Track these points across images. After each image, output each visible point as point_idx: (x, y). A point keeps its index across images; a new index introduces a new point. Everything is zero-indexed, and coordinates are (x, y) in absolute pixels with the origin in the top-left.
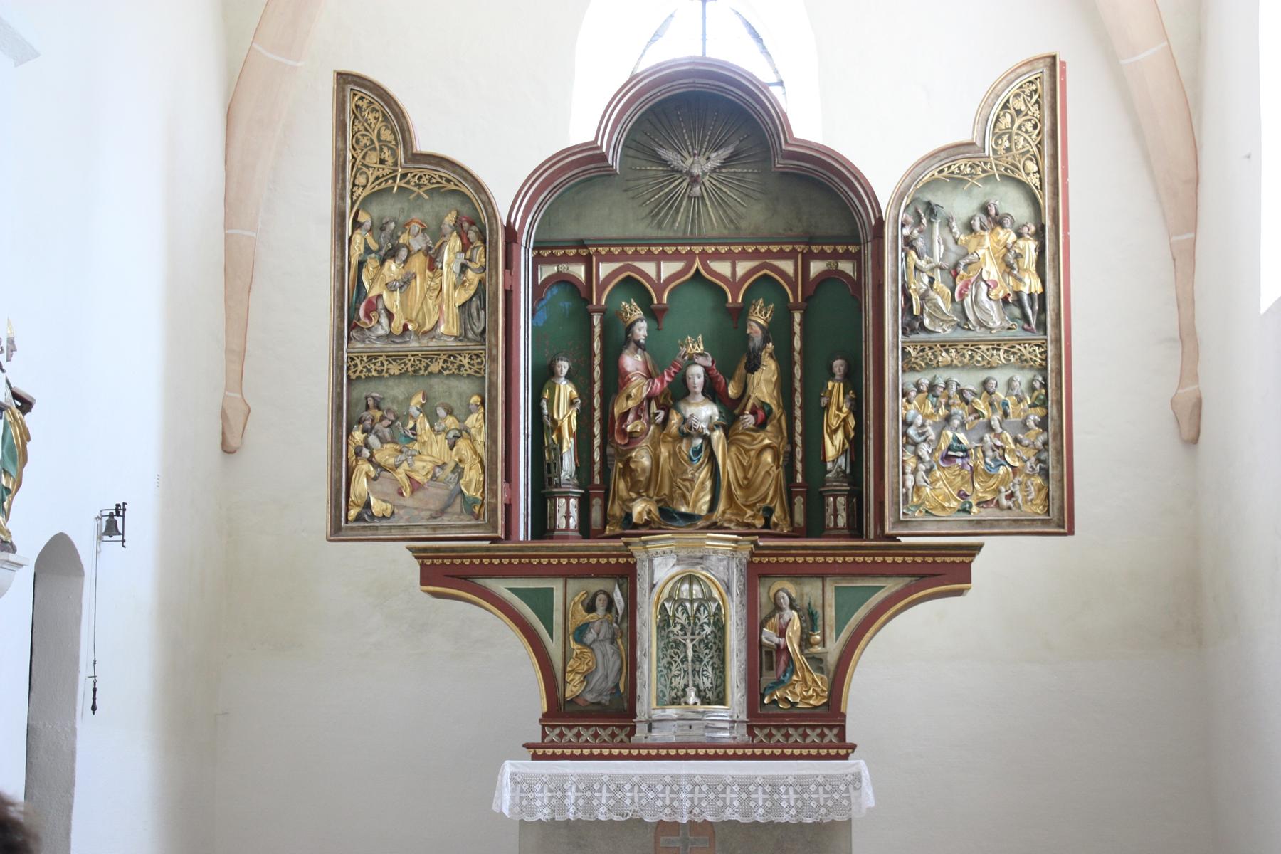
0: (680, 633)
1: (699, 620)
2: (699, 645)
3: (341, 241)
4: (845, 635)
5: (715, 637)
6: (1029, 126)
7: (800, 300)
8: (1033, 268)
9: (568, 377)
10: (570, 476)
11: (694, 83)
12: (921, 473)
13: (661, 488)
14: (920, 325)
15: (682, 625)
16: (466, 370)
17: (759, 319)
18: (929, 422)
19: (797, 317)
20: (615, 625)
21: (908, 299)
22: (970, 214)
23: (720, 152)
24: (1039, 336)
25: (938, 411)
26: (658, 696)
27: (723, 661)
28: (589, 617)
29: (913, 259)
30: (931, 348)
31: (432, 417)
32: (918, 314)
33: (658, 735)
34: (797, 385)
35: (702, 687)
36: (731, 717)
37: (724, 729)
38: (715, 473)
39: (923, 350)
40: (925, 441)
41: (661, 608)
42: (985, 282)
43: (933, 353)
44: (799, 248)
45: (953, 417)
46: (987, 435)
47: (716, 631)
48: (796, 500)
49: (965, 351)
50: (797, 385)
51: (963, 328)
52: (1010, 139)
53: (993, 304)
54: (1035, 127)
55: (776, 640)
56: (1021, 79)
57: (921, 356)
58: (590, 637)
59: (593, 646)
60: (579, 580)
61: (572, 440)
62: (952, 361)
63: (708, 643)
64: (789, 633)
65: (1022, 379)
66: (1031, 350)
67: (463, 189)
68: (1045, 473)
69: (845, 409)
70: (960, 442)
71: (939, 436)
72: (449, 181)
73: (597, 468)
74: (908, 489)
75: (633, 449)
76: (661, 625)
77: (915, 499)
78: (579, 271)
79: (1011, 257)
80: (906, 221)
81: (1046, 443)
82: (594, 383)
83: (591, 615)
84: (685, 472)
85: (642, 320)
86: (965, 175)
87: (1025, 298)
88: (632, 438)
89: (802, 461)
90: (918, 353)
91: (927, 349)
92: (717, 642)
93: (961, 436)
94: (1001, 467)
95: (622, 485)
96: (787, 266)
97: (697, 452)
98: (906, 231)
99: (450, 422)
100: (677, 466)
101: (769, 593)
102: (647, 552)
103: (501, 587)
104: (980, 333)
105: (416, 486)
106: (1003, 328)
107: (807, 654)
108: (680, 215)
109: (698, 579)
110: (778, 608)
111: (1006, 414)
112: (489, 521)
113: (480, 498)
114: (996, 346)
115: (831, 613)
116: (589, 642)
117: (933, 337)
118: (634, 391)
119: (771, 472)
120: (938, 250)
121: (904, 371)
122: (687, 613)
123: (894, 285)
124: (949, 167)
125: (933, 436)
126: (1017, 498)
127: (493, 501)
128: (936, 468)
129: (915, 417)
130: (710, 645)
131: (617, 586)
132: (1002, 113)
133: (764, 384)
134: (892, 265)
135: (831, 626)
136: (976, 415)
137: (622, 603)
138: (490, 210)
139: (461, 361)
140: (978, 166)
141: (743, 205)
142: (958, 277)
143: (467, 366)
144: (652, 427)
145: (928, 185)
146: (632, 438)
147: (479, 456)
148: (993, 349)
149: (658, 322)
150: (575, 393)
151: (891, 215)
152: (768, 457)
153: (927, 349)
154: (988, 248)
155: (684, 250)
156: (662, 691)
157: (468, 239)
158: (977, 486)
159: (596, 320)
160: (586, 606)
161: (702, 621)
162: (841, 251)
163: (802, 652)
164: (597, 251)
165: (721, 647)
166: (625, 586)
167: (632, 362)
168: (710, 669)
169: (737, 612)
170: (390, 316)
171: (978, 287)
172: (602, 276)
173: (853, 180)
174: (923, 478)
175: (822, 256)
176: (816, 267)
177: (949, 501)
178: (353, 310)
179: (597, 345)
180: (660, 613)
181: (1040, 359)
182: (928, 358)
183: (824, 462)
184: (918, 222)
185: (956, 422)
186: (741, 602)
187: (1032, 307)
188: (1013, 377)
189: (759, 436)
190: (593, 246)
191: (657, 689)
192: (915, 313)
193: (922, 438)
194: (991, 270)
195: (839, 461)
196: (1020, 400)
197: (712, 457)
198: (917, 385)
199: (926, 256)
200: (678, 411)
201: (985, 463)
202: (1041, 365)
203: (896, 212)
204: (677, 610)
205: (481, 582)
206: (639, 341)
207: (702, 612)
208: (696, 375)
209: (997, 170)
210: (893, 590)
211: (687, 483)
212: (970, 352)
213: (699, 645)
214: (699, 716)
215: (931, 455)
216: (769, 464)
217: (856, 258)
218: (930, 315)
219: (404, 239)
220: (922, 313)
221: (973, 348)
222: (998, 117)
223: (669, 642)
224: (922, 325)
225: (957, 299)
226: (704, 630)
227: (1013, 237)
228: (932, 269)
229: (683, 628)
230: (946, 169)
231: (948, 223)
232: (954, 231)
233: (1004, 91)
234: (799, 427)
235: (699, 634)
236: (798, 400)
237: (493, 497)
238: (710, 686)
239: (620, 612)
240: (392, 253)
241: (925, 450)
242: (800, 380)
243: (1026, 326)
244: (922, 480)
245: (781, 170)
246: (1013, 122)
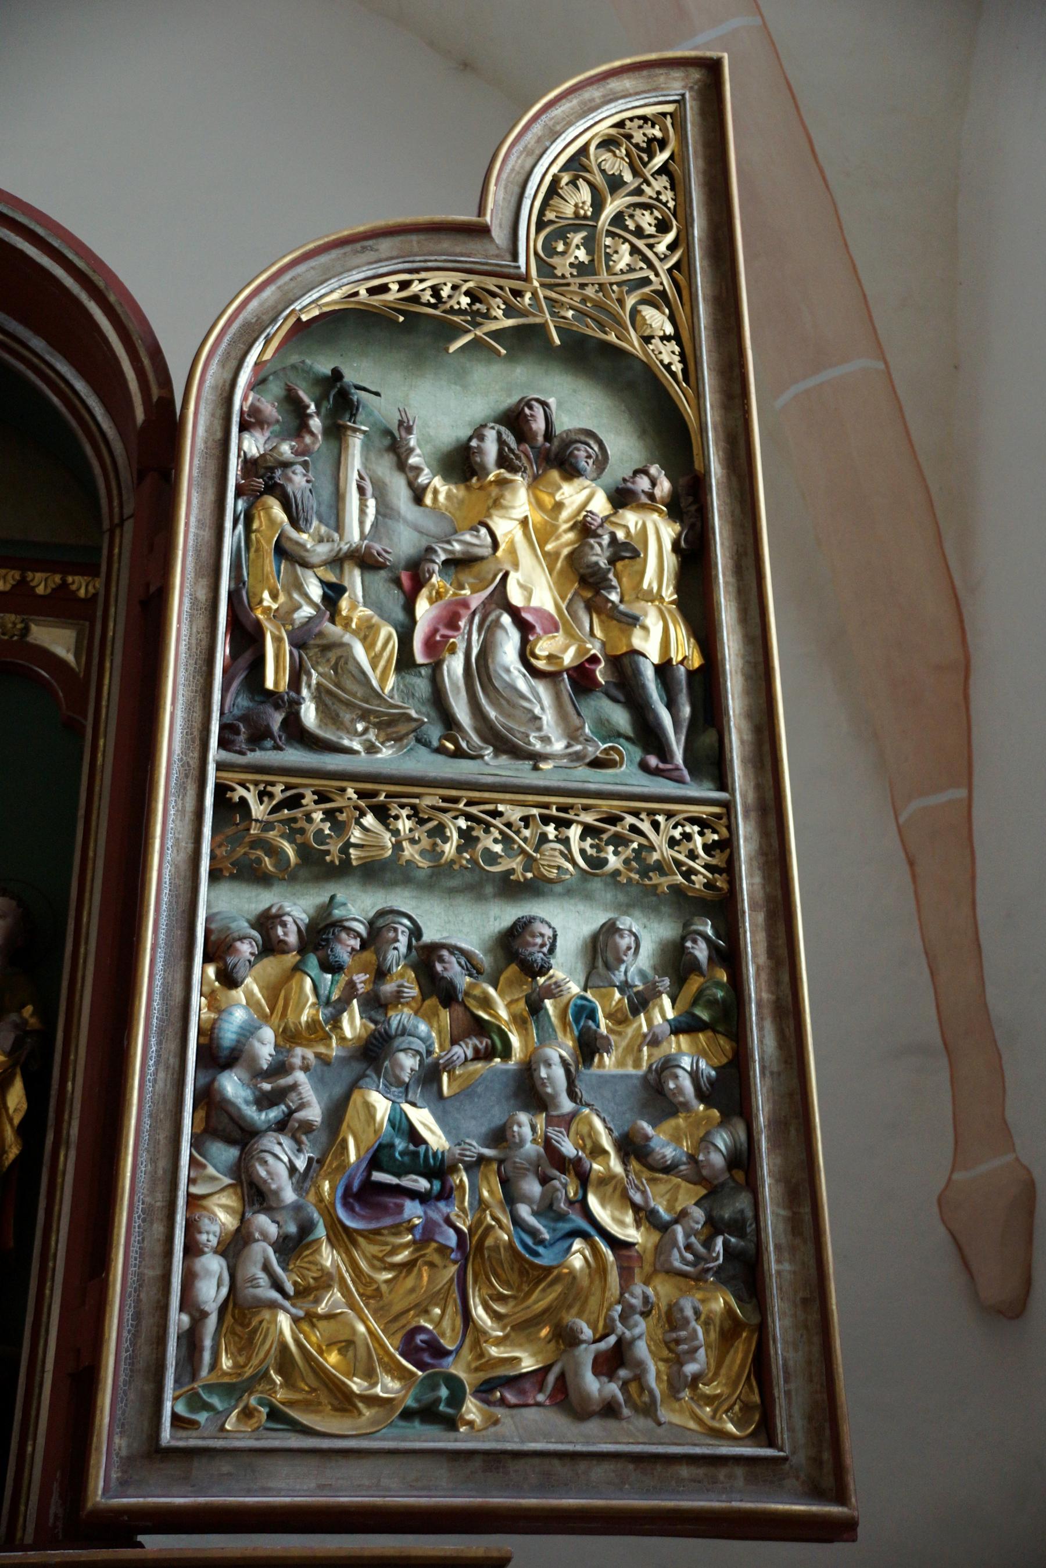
6: (647, 220)
8: (669, 594)
12: (263, 1251)
14: (284, 723)
22: (464, 433)
25: (335, 1022)
29: (272, 521)
30: (322, 798)
39: (294, 802)
40: (281, 1126)
42: (515, 613)
43: (330, 815)
45: (398, 1042)
46: (523, 1117)
49: (446, 818)
51: (441, 750)
52: (589, 244)
53: (542, 688)
54: (663, 227)
56: (620, 105)
62: (398, 847)
66: (677, 833)
70: (414, 1136)
74: (199, 1316)
77: (226, 1363)
79: (599, 555)
80: (255, 411)
86: (452, 311)
87: (649, 674)
90: (275, 810)
91: (309, 799)
93: (422, 1118)
94: (578, 1244)
98: (253, 445)
106: (577, 757)
114: (554, 812)
121: (215, 876)
123: (204, 582)
125: (314, 1113)
126: (639, 1366)
128: (321, 1232)
129: (248, 1032)
132: (566, 178)
134: (201, 524)
136: (482, 1044)
140: (494, 295)
142: (425, 592)
148: (546, 820)
151: (209, 381)
153: (309, 799)
154: (524, 522)
158: (479, 1313)
162: (40, 590)
171: (490, 631)
173: (84, 297)
174: (266, 1268)
177: (370, 1375)
181: (706, 866)
182: (311, 829)
184: (300, 426)
187: (671, 705)
188: (616, 919)
192: (270, 684)
193: (274, 1114)
196: (641, 1003)
199: (315, 523)
201: (517, 1221)
202: (709, 885)
203: (228, 375)
209: (553, 314)
212: (462, 823)
215: (302, 1180)
218: (321, 696)
220: (295, 684)
221: (473, 810)
222: (556, 181)
225: (420, 658)
227: (600, 505)
228: (337, 562)
230: (395, 287)
232: (413, 460)
233: (570, 124)
243: (653, 761)
244: (263, 1279)
246: (598, 205)
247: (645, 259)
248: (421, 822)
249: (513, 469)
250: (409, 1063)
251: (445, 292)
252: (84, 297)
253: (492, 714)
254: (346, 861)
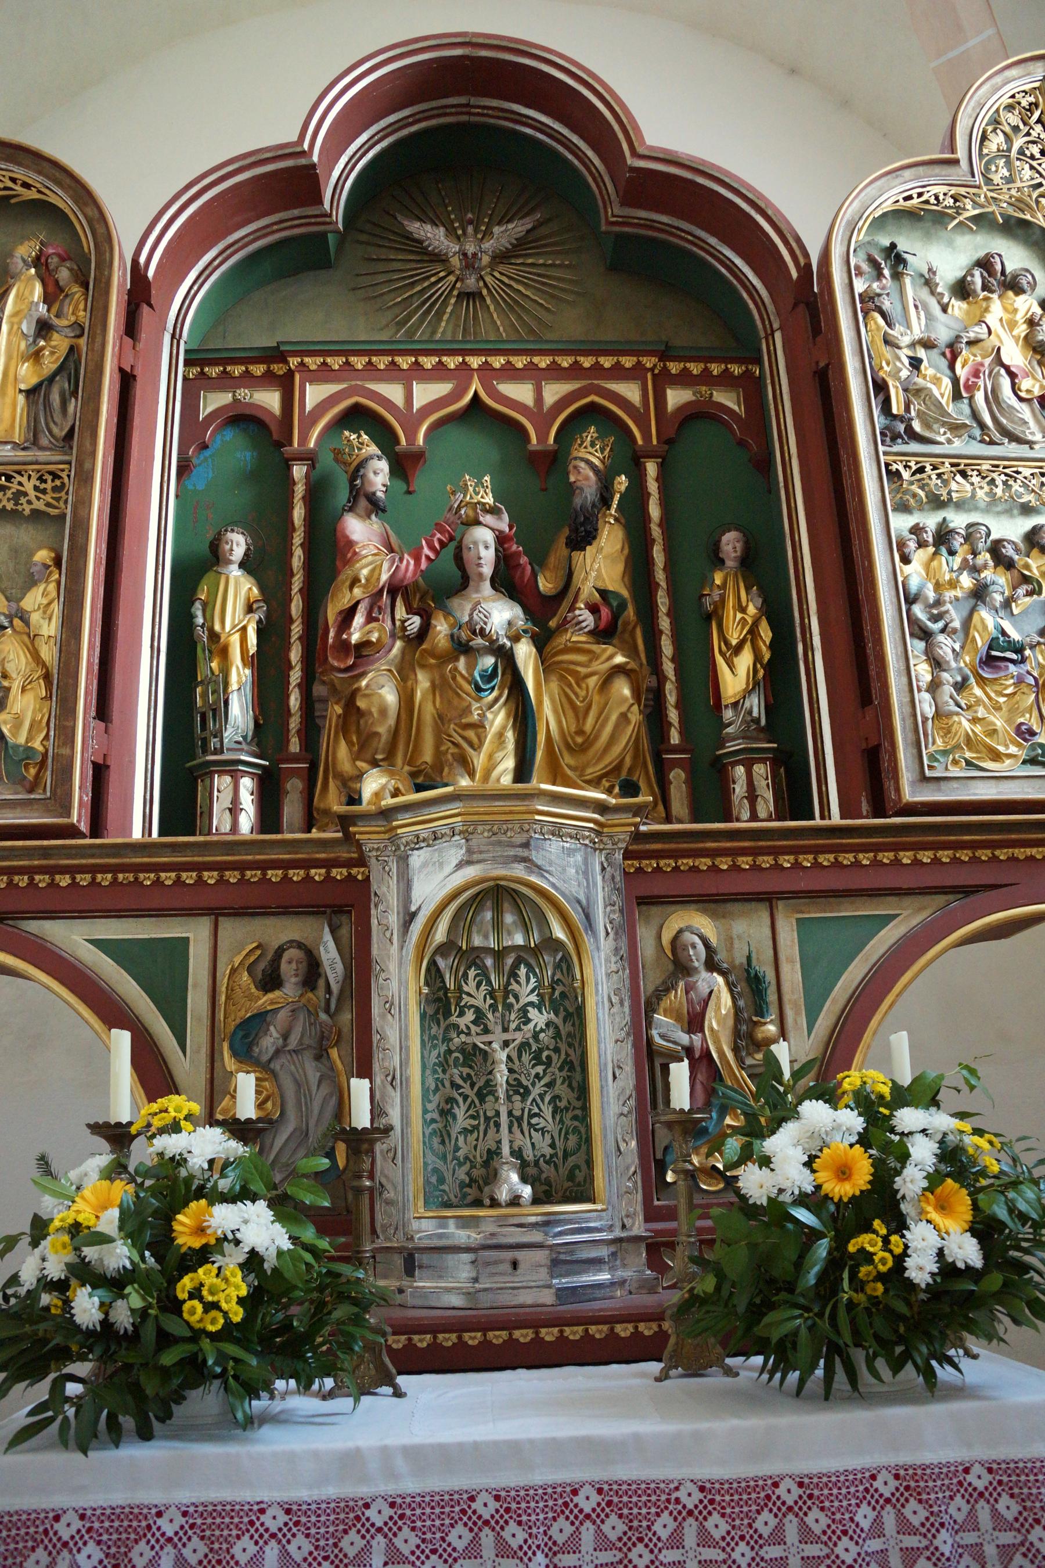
0: (473, 1028)
1: (517, 998)
2: (520, 1057)
4: (825, 1021)
5: (557, 1035)
7: (655, 442)
10: (245, 737)
11: (467, 105)
12: (948, 690)
13: (417, 749)
15: (478, 1011)
16: (29, 502)
18: (949, 594)
20: (323, 1016)
21: (881, 387)
22: (960, 274)
23: (510, 226)
26: (427, 1182)
27: (583, 1091)
28: (265, 1001)
32: (902, 412)
34: (660, 576)
35: (529, 1154)
36: (611, 1228)
37: (596, 1263)
39: (921, 470)
40: (943, 631)
41: (428, 970)
42: (1007, 369)
43: (939, 476)
44: (649, 362)
45: (991, 588)
47: (558, 1021)
48: (671, 776)
49: (995, 475)
50: (660, 576)
51: (982, 441)
55: (684, 1038)
57: (919, 480)
58: (269, 1041)
59: (276, 1065)
60: (245, 920)
61: (248, 672)
63: (540, 1051)
64: (712, 1021)
67: (53, 199)
69: (752, 610)
70: (1004, 633)
71: (967, 623)
72: (26, 185)
73: (294, 723)
75: (363, 674)
76: (430, 1011)
78: (270, 400)
82: (292, 575)
83: (270, 996)
84: (468, 710)
85: (379, 458)
86: (946, 207)
89: (677, 706)
90: (913, 474)
92: (563, 1047)
95: (343, 751)
96: (631, 392)
98: (860, 286)
100: (450, 702)
101: (659, 937)
102: (394, 839)
107: (751, 1066)
108: (443, 324)
109: (514, 896)
110: (681, 968)
112: (54, 792)
113: (41, 749)
115: (792, 975)
116: (265, 1058)
118: (365, 572)
119: (629, 715)
122: (489, 983)
124: (920, 195)
125: (957, 624)
127: (65, 751)
128: (972, 680)
130: (545, 1054)
131: (327, 929)
135: (796, 1004)
136: (1030, 587)
137: (340, 967)
138: (101, 230)
139: (20, 484)
141: (547, 309)
143: (32, 494)
144: (399, 644)
145: (881, 222)
147: (44, 665)
149: (408, 483)
150: (255, 591)
152: (625, 690)
153: (928, 468)
155: (451, 362)
156: (436, 1170)
157: (57, 282)
159: (298, 471)
160: (260, 976)
161: (523, 1001)
163: (740, 1061)
164: (302, 364)
165: (574, 1057)
166: (344, 931)
168: (547, 1111)
169: (608, 975)
171: (994, 377)
172: (309, 406)
173: (753, 213)
174: (951, 697)
175: (684, 379)
176: (676, 397)
177: (1007, 746)
179: (298, 513)
180: (427, 984)
183: (718, 706)
184: (880, 275)
186: (617, 950)
189: (604, 650)
190: (295, 353)
191: (425, 1164)
192: (895, 411)
193: (940, 625)
195: (747, 704)
197: (516, 685)
200: (448, 614)
204: (465, 975)
205: (33, 926)
206: (374, 494)
207: (523, 979)
210: (915, 922)
211: (471, 734)
212: (1003, 478)
213: (520, 1057)
214: (536, 1237)
216: (625, 699)
220: (907, 409)
221: (1007, 471)
222: (984, 132)
223: (449, 1052)
224: (909, 430)
226: (529, 1020)
228: (913, 345)
229: (480, 1017)
232: (939, 290)
234: (667, 647)
235: (518, 1029)
236: (662, 601)
237: (65, 744)
238: (548, 1151)
239: (335, 988)
241: (946, 645)
242: (664, 569)
244: (951, 702)
245: (617, 229)
247: (1038, 172)
248: (983, 478)
249: (992, 292)
250: (998, 598)
251: (941, 197)
252: (753, 213)
253: (1004, 421)
254: (950, 499)
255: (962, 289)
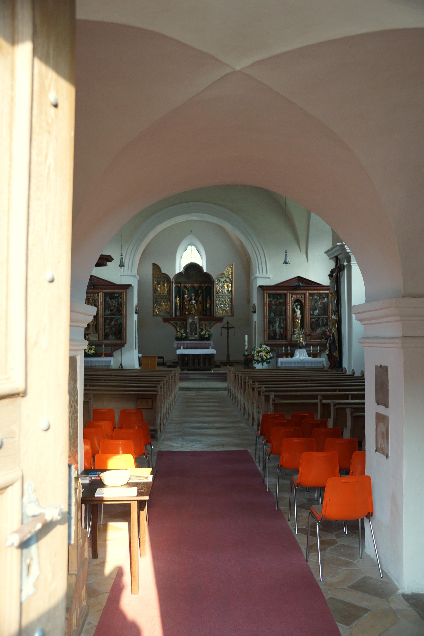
3: (153, 283)
9: (179, 298)
12: (218, 310)
17: (200, 291)
19: (204, 291)
21: (217, 290)
24: (231, 295)
28: (182, 325)
31: (164, 303)
33: (190, 338)
38: (195, 309)
65: (229, 299)
68: (231, 310)
78: (179, 285)
81: (232, 307)
88: (186, 305)
96: (203, 285)
97: (193, 306)
99: (166, 303)
103: (172, 322)
104: (224, 294)
105: (162, 311)
111: (227, 303)
115: (208, 325)
117: (219, 295)
120: (220, 285)
133: (200, 299)
146: (186, 305)
152: (201, 307)
155: (191, 283)
159: (181, 291)
167: (186, 296)
170: (159, 291)
176: (206, 285)
178: (155, 290)
184: (218, 282)
185: (222, 304)
194: (226, 287)
198: (218, 300)
200: (191, 302)
208: (193, 297)
217: (211, 284)
219: (160, 282)
227: (228, 283)
231: (221, 282)
240: (159, 284)
241: (219, 307)
255: (223, 282)
